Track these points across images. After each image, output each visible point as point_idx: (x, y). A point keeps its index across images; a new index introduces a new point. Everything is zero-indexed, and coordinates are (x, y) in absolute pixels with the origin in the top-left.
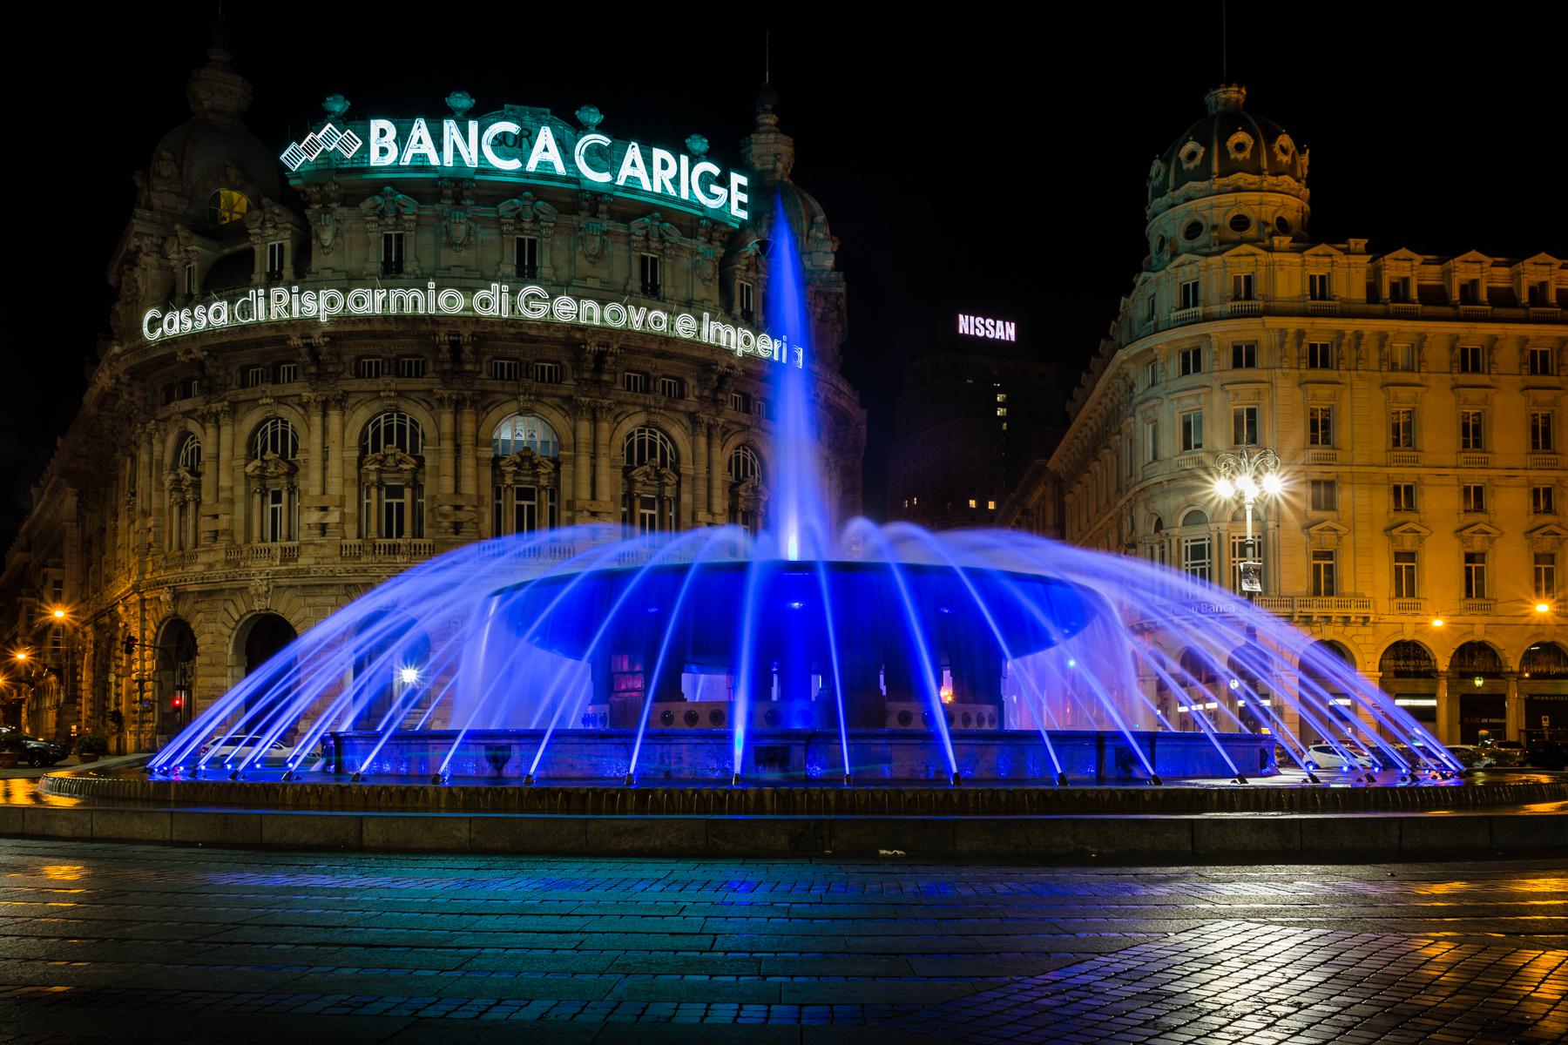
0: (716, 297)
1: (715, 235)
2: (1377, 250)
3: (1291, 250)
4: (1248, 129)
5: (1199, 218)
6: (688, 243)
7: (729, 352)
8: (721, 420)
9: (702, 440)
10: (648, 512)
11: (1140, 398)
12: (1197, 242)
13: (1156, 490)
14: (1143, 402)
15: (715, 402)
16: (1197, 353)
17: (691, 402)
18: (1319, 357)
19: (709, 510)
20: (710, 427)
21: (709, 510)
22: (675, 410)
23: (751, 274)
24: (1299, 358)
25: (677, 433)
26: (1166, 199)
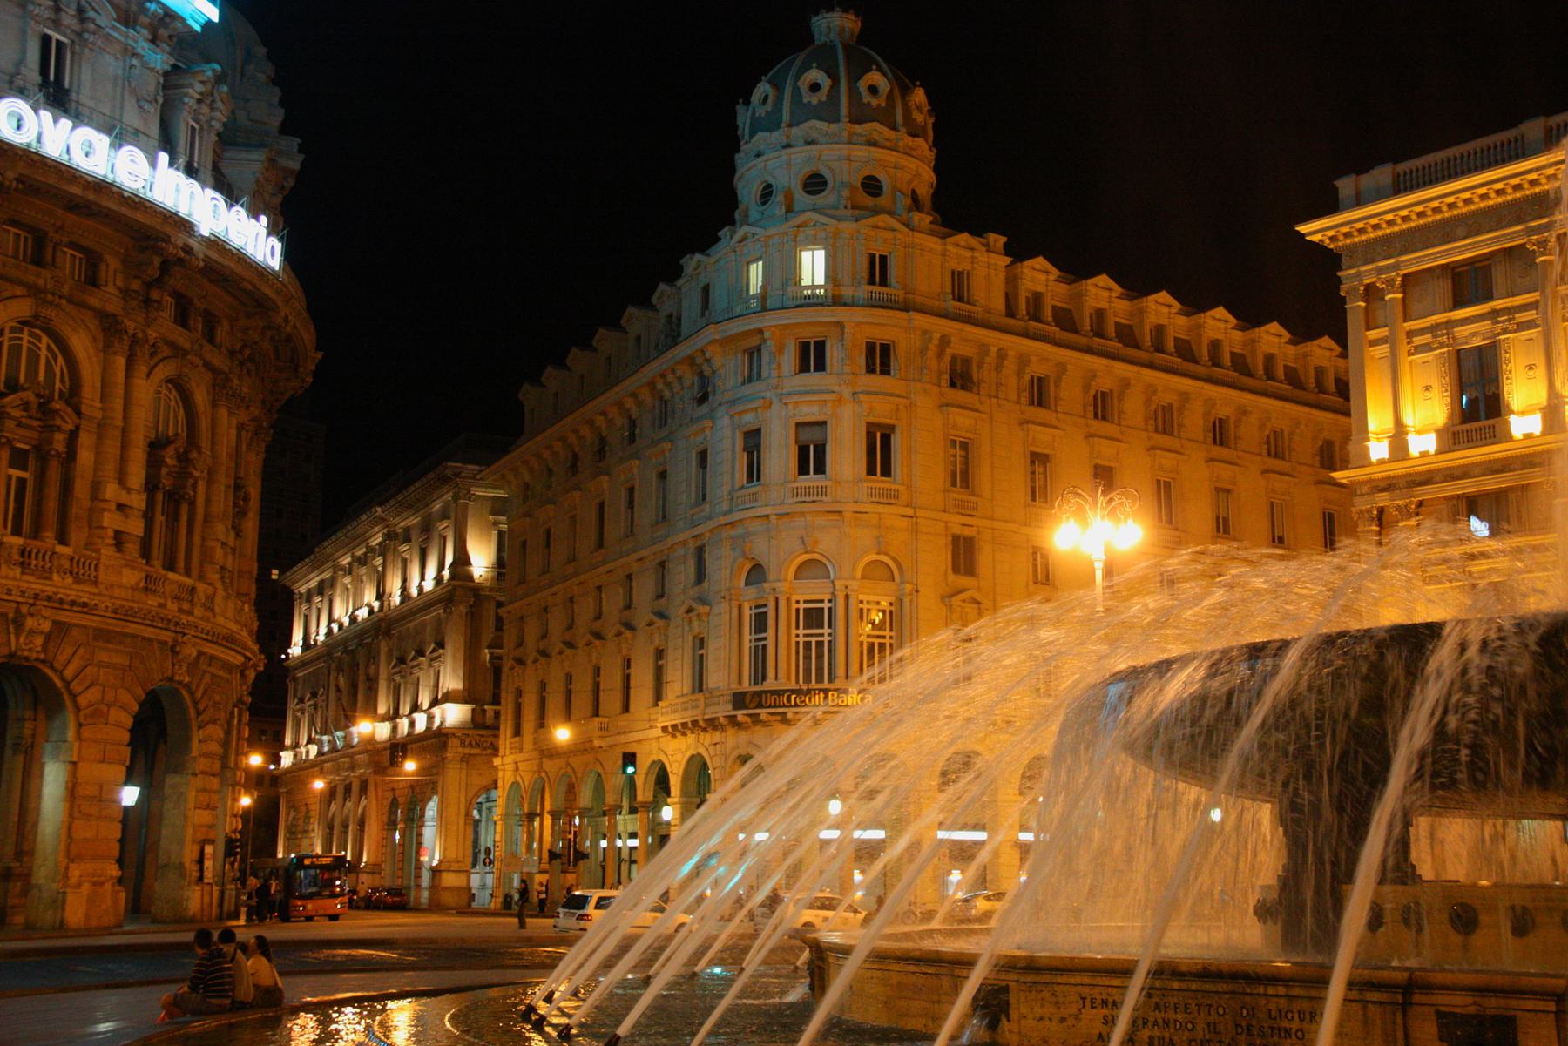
0: (155, 130)
1: (163, 32)
2: (1018, 252)
3: (932, 233)
4: (879, 69)
5: (824, 171)
6: (119, 33)
7: (186, 226)
8: (153, 334)
9: (121, 361)
10: (15, 473)
11: (727, 397)
12: (820, 200)
13: (757, 526)
14: (733, 402)
15: (147, 302)
16: (820, 346)
17: (108, 297)
18: (960, 377)
19: (122, 481)
20: (134, 341)
21: (122, 481)
22: (83, 305)
23: (205, 109)
24: (940, 373)
25: (82, 344)
26: (777, 136)
